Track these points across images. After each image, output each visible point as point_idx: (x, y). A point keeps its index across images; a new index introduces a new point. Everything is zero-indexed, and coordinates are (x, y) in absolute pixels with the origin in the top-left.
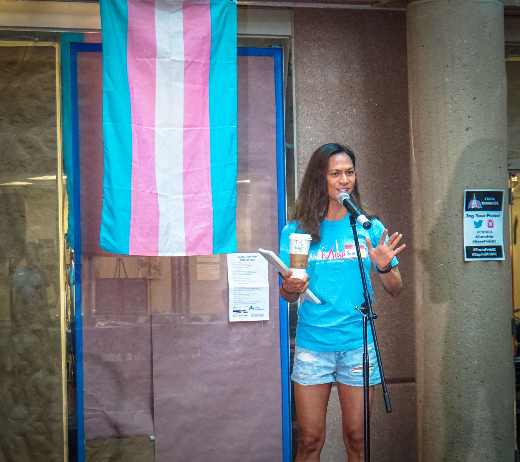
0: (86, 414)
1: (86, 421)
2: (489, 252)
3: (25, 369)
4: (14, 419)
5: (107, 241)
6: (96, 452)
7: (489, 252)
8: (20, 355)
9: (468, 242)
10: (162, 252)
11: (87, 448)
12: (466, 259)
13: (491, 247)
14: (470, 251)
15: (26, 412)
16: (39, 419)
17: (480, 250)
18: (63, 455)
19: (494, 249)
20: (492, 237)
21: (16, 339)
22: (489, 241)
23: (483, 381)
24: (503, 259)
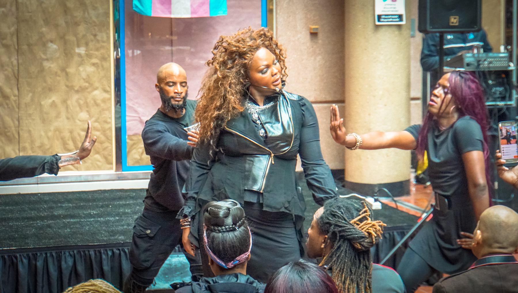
0: (127, 118)
1: (127, 124)
2: (393, 18)
3: (87, 89)
4: (80, 121)
5: (137, 7)
6: (134, 144)
7: (393, 18)
8: (84, 79)
9: (378, 12)
10: (173, 14)
11: (128, 141)
12: (377, 23)
13: (395, 15)
14: (379, 17)
15: (88, 116)
16: (96, 121)
17: (387, 17)
18: (112, 144)
19: (396, 17)
20: (395, 8)
21: (81, 69)
22: (392, 11)
23: (385, 105)
24: (403, 23)
